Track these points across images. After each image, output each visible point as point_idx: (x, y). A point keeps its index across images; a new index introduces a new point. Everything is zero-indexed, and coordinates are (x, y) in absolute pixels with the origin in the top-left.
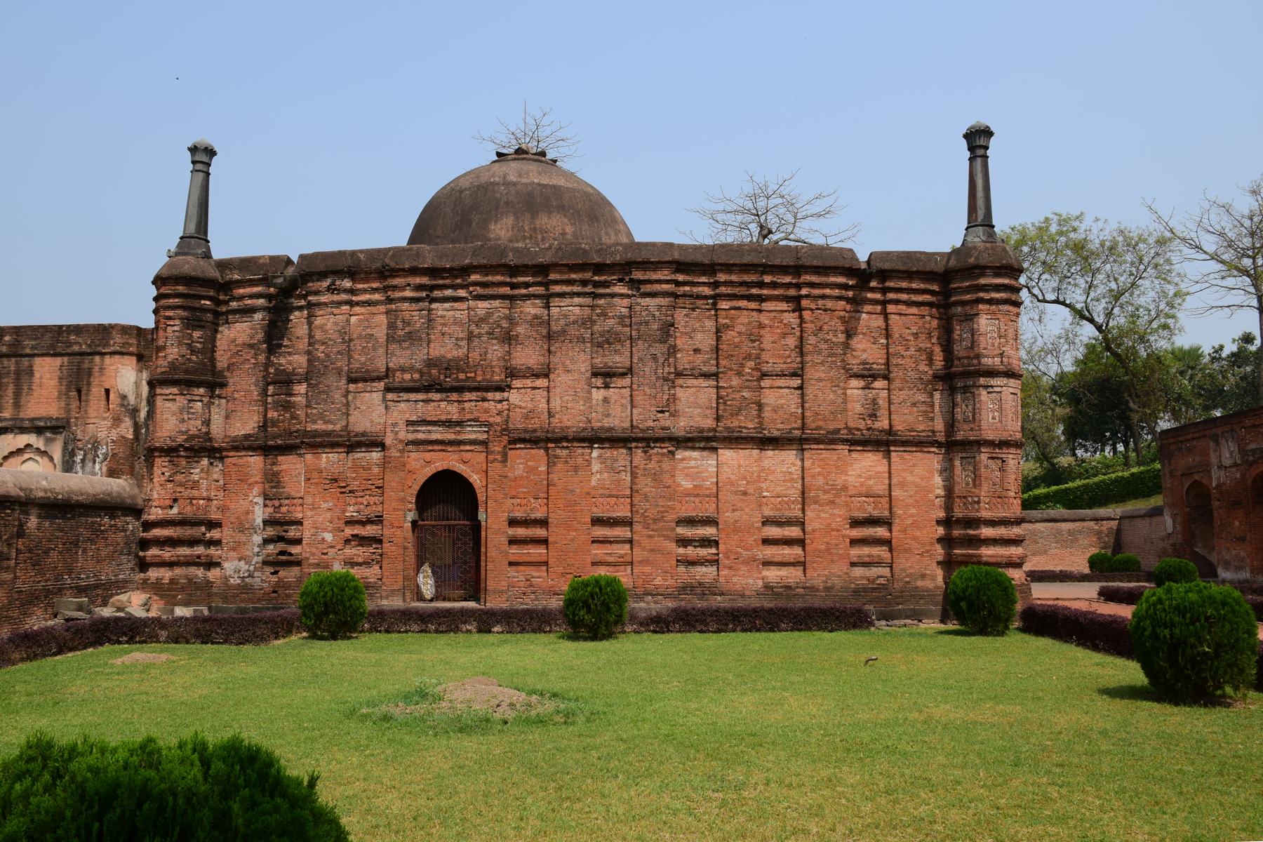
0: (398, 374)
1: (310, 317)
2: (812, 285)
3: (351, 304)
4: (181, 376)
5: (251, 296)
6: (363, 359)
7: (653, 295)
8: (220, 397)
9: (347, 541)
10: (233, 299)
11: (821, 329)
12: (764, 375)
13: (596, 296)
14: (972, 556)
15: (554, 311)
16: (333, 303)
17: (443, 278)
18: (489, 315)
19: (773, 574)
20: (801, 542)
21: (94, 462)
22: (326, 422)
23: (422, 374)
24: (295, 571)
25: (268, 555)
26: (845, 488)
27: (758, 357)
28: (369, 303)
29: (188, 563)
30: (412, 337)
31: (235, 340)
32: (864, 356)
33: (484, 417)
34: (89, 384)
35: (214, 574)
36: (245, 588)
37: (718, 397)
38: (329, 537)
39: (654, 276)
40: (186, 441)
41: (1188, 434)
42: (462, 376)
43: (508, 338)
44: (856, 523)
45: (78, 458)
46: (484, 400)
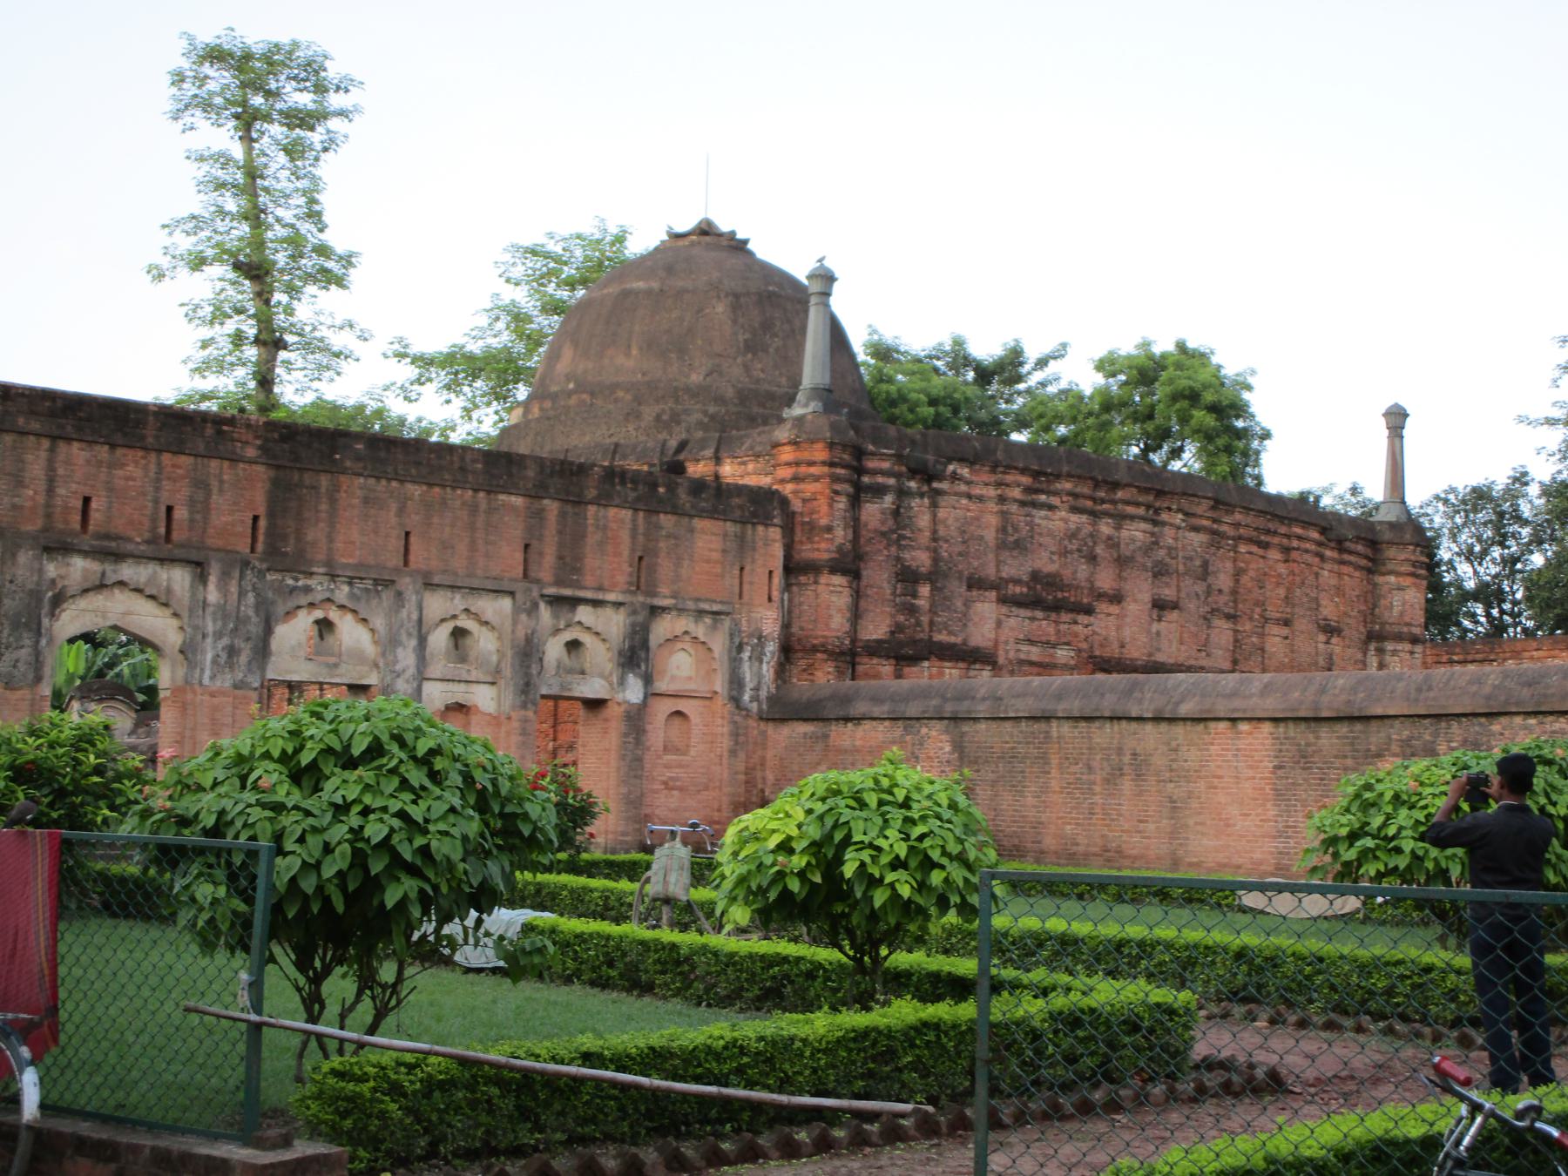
0: (1011, 586)
1: (934, 505)
2: (1300, 538)
3: (969, 497)
7: (1196, 529)
12: (1267, 620)
15: (1124, 533)
21: (761, 662)
22: (951, 633)
23: (1029, 588)
30: (1019, 546)
34: (753, 561)
37: (1236, 641)
45: (746, 655)
46: (1076, 623)
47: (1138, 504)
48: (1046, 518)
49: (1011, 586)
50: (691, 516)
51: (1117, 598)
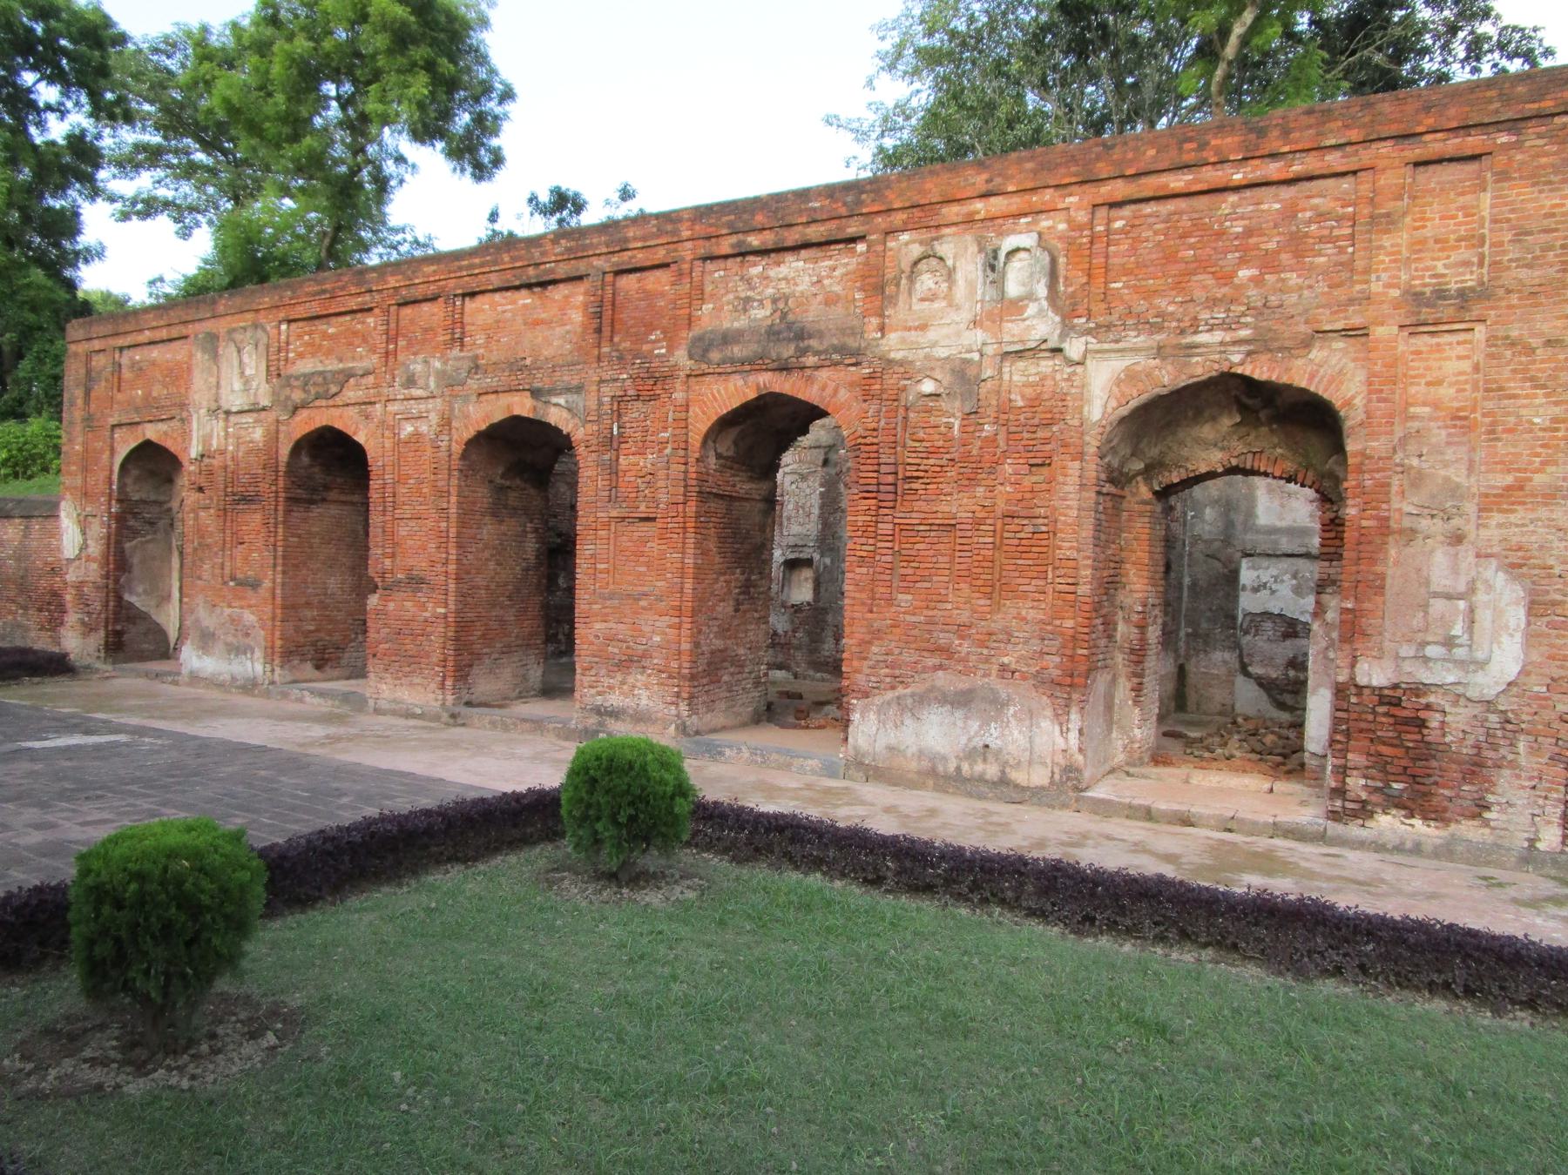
41: (141, 331)
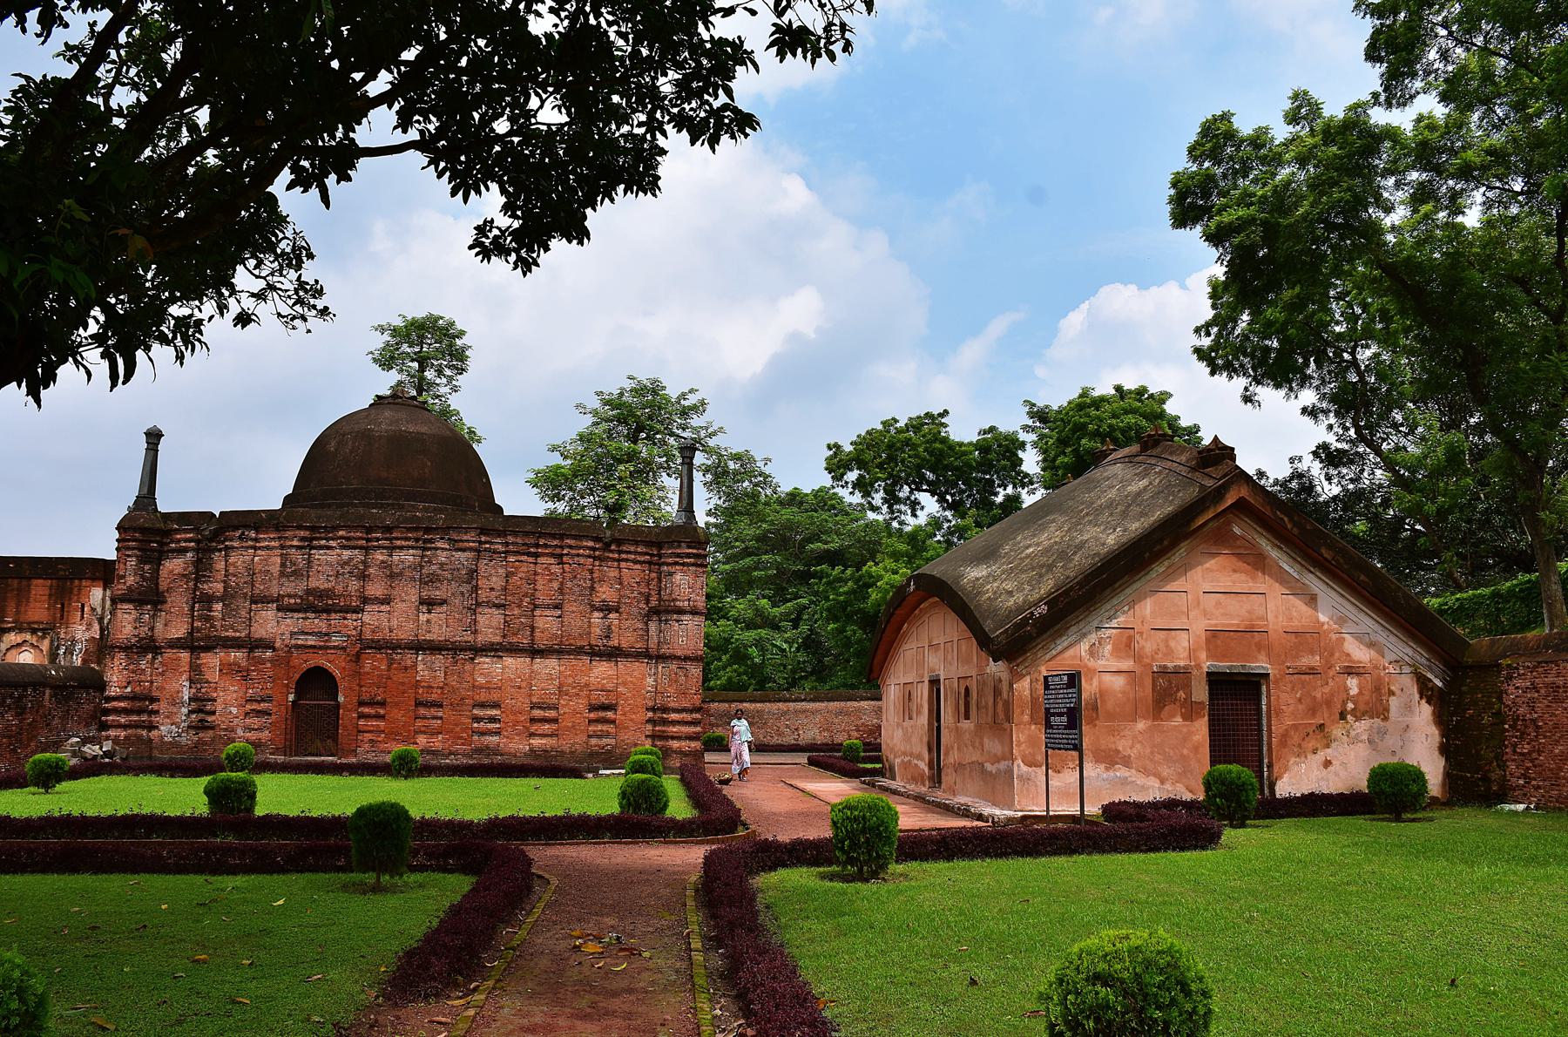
0: (286, 599)
2: (571, 547)
3: (255, 548)
4: (136, 596)
5: (186, 540)
6: (262, 587)
7: (464, 550)
8: (161, 610)
9: (247, 714)
10: (172, 542)
11: (575, 577)
12: (536, 607)
13: (425, 549)
14: (664, 731)
15: (396, 558)
16: (242, 547)
17: (320, 533)
18: (351, 559)
19: (536, 742)
20: (555, 721)
22: (235, 631)
24: (210, 733)
25: (192, 722)
26: (587, 685)
27: (533, 595)
28: (267, 548)
29: (137, 726)
30: (297, 574)
31: (172, 571)
32: (604, 596)
33: (344, 631)
34: (70, 599)
35: (154, 733)
36: (174, 744)
38: (234, 710)
39: (465, 538)
40: (137, 641)
42: (330, 602)
43: (363, 577)
44: (593, 708)
45: (61, 652)
46: (345, 619)
47: (407, 539)
48: (325, 553)
49: (286, 599)
50: (30, 579)
51: (386, 601)
